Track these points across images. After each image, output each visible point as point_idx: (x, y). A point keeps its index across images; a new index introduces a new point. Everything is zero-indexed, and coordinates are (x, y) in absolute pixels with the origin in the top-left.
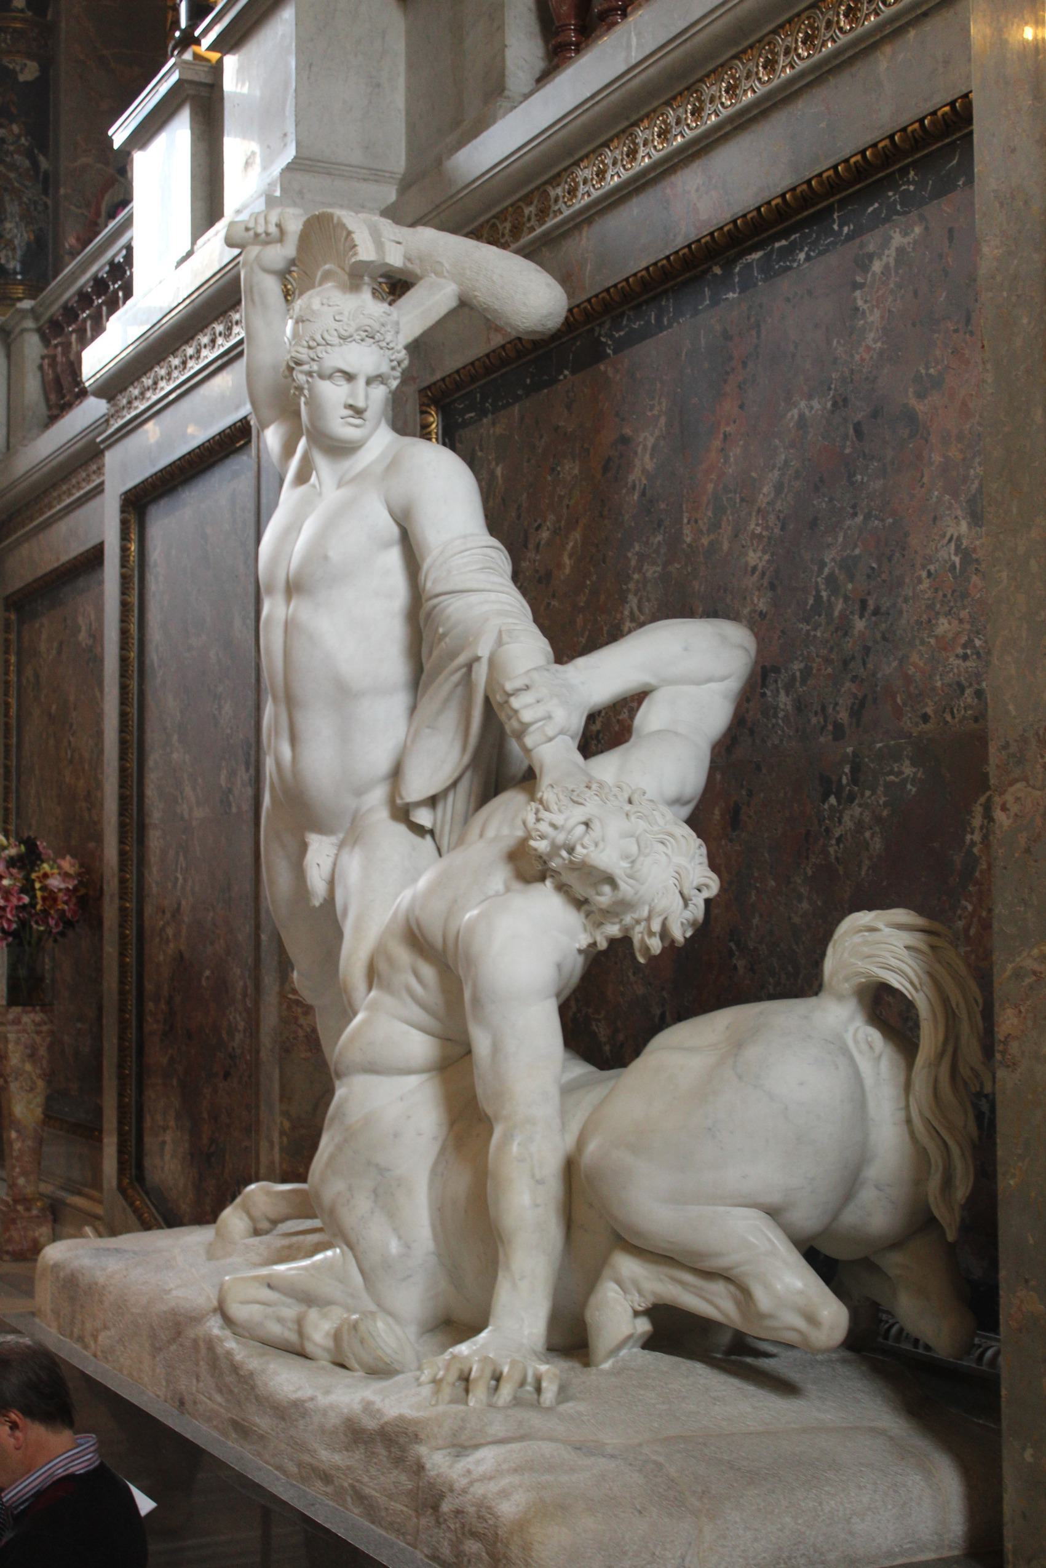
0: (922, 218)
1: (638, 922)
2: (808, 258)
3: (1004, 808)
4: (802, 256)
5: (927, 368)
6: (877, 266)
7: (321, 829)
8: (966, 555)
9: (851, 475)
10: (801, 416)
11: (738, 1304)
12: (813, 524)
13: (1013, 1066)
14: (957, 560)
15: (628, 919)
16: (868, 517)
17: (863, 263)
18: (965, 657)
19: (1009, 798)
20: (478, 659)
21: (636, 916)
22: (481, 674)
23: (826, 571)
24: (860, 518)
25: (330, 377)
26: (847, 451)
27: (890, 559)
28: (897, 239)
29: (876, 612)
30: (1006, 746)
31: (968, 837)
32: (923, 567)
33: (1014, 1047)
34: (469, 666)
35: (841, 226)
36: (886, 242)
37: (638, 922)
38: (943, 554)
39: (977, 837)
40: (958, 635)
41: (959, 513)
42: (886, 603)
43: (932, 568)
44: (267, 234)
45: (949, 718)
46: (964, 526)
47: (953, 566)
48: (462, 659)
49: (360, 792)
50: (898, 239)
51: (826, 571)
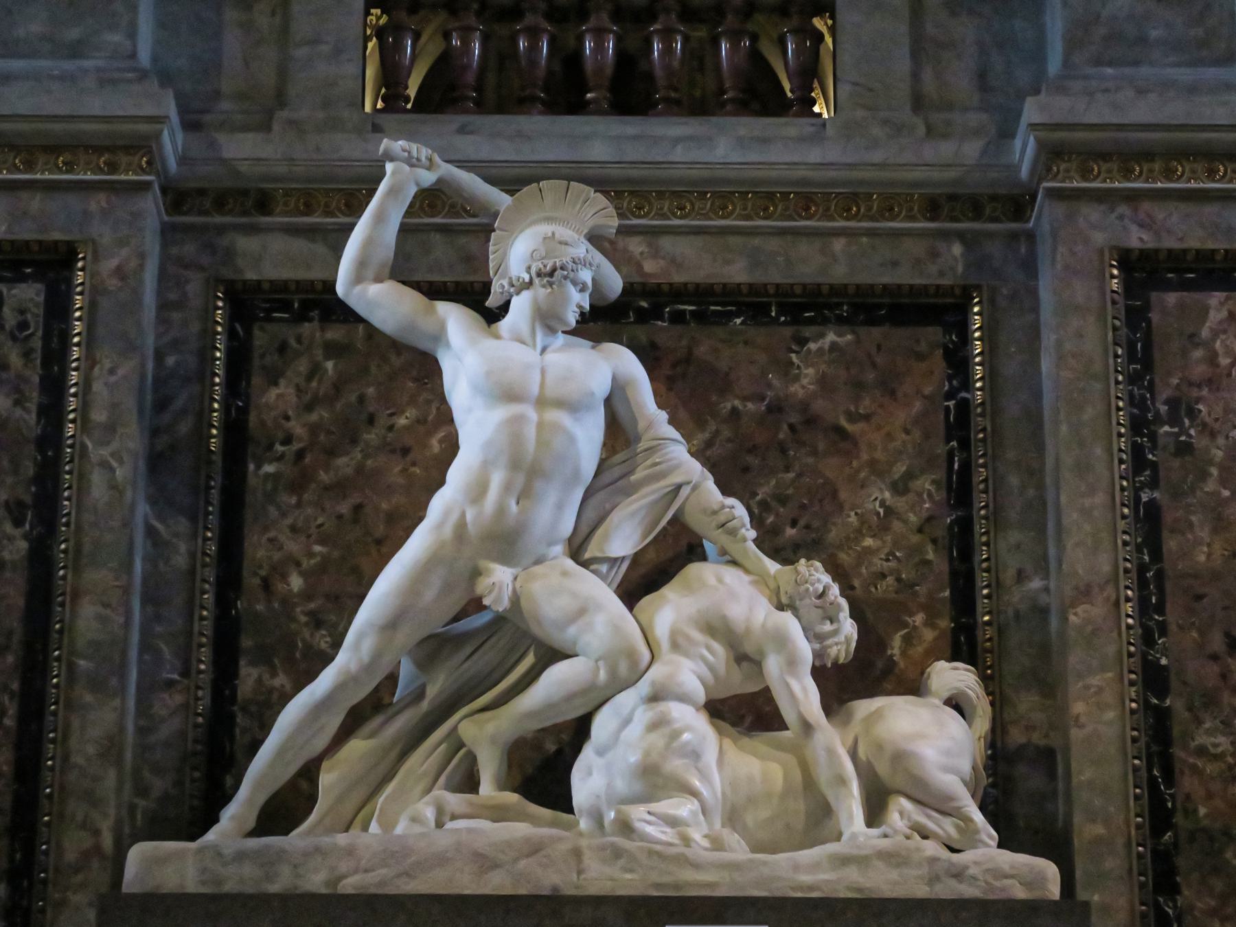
0: (853, 332)
1: (837, 644)
2: (741, 324)
3: (1075, 614)
4: (738, 321)
5: (857, 408)
6: (813, 346)
7: (506, 558)
8: (889, 511)
9: (783, 451)
10: (734, 410)
11: (957, 827)
12: (746, 469)
13: (1082, 727)
14: (881, 511)
15: (829, 642)
16: (799, 475)
17: (802, 342)
18: (887, 560)
19: (1079, 610)
20: (688, 483)
21: (836, 640)
22: (685, 491)
23: (758, 498)
24: (791, 475)
25: (575, 283)
26: (781, 436)
27: (821, 501)
28: (831, 337)
29: (807, 527)
30: (1077, 588)
31: (889, 652)
32: (852, 510)
33: (1083, 719)
34: (679, 487)
35: (779, 314)
36: (822, 335)
37: (837, 644)
38: (870, 506)
39: (896, 651)
40: (878, 550)
41: (883, 486)
42: (816, 524)
43: (859, 511)
44: (418, 160)
45: (873, 590)
46: (887, 495)
47: (878, 513)
48: (676, 479)
49: (550, 544)
50: (831, 337)
51: (758, 498)
